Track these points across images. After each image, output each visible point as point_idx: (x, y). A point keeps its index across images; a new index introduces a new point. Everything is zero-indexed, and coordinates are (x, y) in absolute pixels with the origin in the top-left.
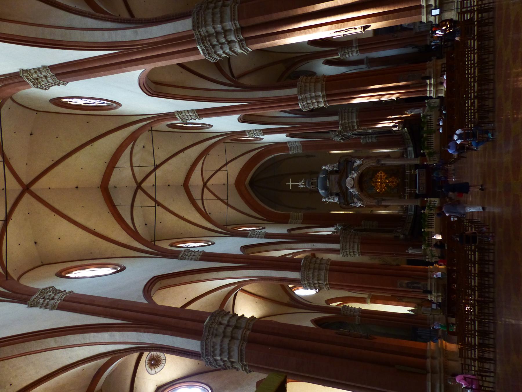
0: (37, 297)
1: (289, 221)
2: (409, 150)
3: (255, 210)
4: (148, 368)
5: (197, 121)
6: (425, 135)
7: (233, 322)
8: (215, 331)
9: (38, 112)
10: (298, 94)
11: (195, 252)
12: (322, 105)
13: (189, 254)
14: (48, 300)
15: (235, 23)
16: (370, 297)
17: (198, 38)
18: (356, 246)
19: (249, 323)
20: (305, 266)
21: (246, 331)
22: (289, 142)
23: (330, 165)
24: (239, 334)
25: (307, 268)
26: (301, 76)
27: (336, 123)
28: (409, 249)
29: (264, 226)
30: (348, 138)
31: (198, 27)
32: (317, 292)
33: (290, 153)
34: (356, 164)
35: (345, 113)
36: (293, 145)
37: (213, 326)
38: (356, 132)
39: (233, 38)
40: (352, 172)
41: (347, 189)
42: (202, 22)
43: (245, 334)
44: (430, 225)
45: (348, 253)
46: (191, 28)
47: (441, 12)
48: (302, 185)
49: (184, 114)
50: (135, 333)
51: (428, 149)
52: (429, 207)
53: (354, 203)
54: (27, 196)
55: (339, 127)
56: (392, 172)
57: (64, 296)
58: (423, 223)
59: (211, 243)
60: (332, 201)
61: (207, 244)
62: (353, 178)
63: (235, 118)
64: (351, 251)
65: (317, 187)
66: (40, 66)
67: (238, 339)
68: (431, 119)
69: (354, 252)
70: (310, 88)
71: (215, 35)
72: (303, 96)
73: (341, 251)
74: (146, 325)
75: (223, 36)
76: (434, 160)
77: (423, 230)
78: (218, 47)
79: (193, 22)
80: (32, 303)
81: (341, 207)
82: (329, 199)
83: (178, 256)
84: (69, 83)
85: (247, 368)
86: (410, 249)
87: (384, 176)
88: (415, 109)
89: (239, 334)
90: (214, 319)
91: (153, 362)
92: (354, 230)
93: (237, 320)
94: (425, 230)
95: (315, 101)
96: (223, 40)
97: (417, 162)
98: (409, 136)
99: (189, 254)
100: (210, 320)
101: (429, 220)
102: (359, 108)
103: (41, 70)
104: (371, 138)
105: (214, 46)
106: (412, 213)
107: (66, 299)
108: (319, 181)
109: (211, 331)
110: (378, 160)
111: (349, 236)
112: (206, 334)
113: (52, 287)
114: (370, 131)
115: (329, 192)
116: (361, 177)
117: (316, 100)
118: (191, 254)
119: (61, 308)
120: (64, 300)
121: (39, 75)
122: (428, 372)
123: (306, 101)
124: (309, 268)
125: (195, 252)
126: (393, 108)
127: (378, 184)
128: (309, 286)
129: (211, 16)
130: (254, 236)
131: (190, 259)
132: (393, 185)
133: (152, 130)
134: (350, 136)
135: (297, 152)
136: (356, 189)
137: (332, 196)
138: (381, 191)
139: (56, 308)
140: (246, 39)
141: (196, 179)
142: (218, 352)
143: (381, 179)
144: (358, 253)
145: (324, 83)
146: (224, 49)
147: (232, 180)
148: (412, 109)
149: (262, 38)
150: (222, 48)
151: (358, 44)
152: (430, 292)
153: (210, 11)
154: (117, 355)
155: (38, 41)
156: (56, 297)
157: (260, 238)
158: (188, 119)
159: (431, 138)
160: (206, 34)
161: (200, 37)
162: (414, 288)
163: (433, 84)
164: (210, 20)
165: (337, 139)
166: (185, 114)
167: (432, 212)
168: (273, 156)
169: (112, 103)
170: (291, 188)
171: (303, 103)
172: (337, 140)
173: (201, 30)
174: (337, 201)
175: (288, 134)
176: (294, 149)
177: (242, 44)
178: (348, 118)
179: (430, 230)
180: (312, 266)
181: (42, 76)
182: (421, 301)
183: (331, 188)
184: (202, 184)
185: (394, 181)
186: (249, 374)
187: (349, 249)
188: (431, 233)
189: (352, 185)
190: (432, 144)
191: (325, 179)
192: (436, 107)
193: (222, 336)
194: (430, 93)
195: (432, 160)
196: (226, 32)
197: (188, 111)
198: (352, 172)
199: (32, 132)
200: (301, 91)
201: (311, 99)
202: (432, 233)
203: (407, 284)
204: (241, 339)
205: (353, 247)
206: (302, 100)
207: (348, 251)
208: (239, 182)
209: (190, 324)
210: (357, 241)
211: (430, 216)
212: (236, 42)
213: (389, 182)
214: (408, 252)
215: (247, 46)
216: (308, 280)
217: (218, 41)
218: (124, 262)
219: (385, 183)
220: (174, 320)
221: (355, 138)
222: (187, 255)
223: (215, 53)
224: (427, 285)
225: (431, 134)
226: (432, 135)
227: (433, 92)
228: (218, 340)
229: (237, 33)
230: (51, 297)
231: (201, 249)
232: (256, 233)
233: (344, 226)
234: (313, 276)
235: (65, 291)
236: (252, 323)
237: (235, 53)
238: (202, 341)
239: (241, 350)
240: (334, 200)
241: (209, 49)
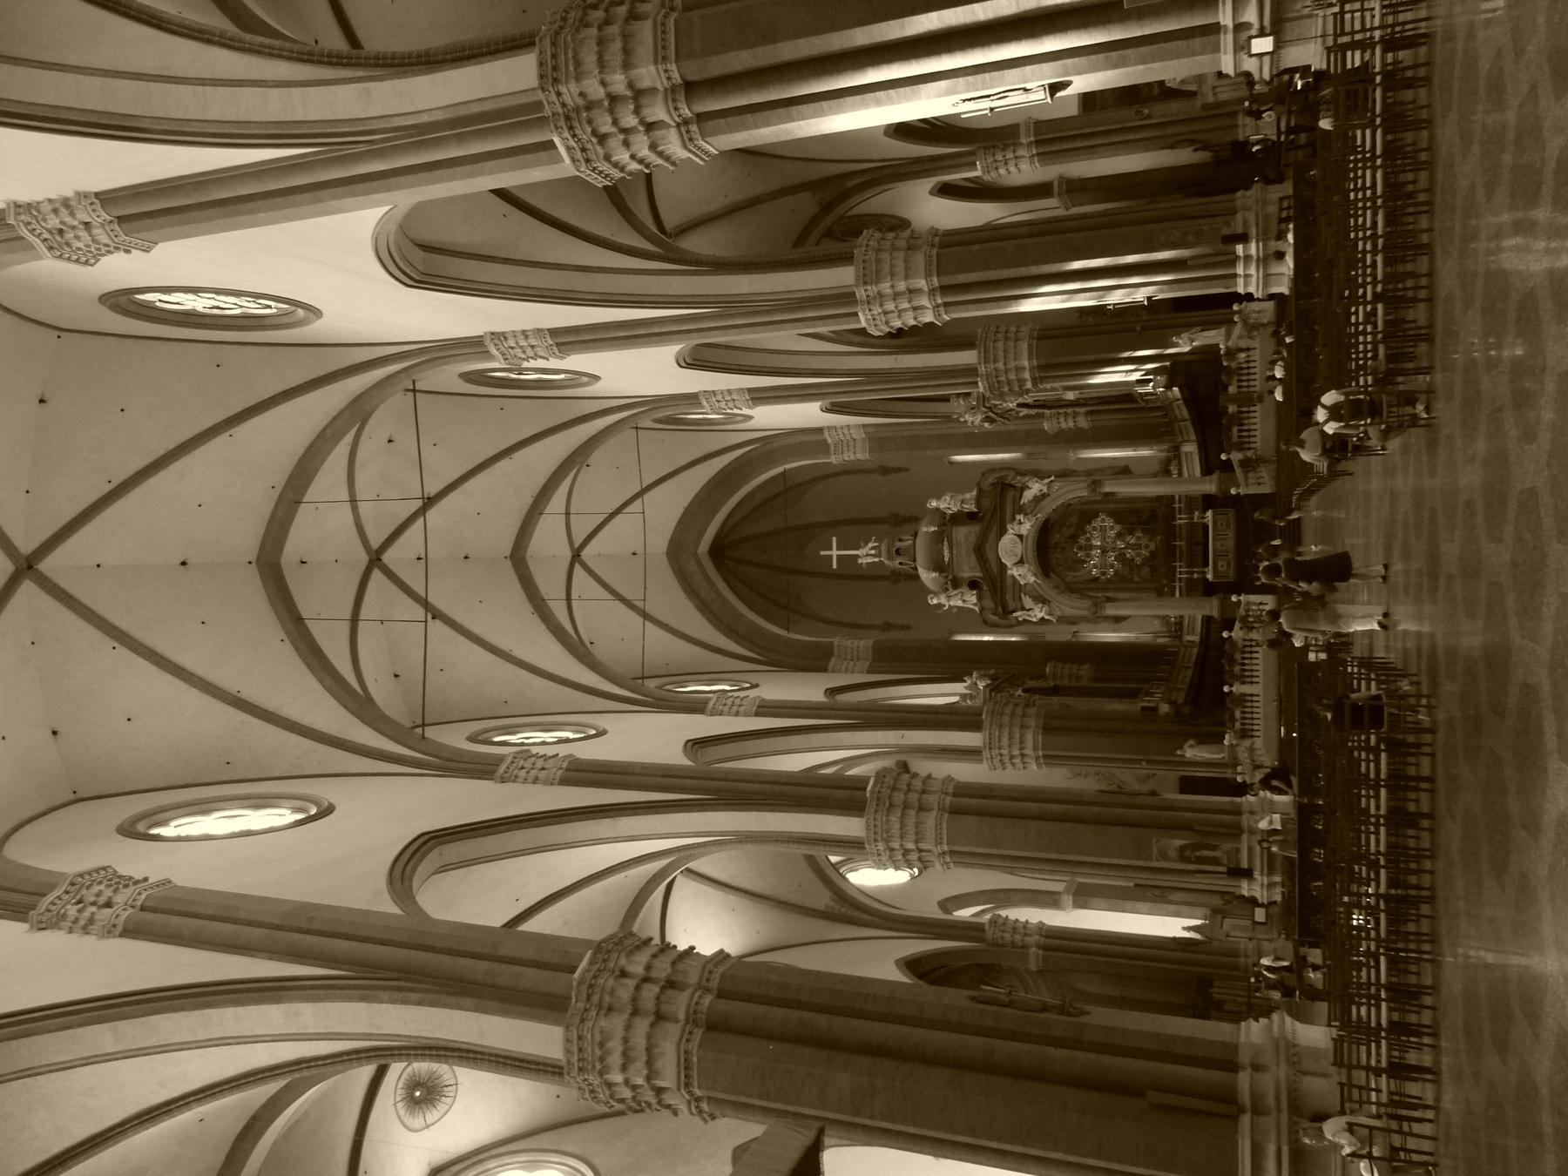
0: (59, 898)
1: (831, 664)
2: (1186, 453)
3: (729, 631)
4: (402, 1112)
5: (553, 363)
6: (1232, 409)
7: (662, 969)
8: (607, 998)
9: (62, 334)
10: (857, 285)
11: (545, 760)
12: (928, 317)
13: (528, 764)
14: (93, 909)
15: (666, 71)
16: (1073, 890)
17: (554, 114)
18: (1029, 737)
19: (710, 972)
20: (878, 799)
21: (700, 997)
22: (829, 428)
23: (952, 497)
24: (680, 1004)
26: (865, 231)
27: (970, 371)
28: (1186, 746)
29: (754, 678)
30: (1005, 415)
31: (556, 81)
32: (913, 878)
33: (833, 459)
34: (1028, 496)
35: (995, 341)
36: (842, 437)
37: (602, 981)
38: (1029, 399)
39: (657, 111)
40: (1018, 517)
41: (1003, 567)
42: (567, 68)
43: (697, 1003)
44: (1247, 674)
45: (1006, 759)
46: (535, 83)
47: (1278, 45)
48: (868, 555)
49: (512, 343)
50: (362, 1006)
51: (1241, 449)
52: (1244, 620)
53: (1023, 609)
54: (28, 588)
55: (980, 384)
56: (1137, 516)
57: (143, 896)
58: (1227, 669)
59: (594, 732)
60: (960, 603)
61: (582, 735)
62: (1020, 537)
63: (668, 353)
64: (1016, 752)
65: (915, 561)
66: (70, 194)
67: (677, 1021)
68: (1248, 362)
69: (1023, 755)
70: (892, 266)
71: (606, 103)
72: (873, 289)
73: (986, 754)
74: (398, 980)
75: (632, 107)
76: (1259, 481)
77: (1226, 689)
78: (615, 142)
79: (541, 64)
80: (44, 919)
81: (985, 622)
82: (949, 597)
83: (495, 772)
84: (161, 245)
85: (705, 1106)
86: (1191, 746)
87: (1112, 528)
88: (1202, 331)
89: (680, 1004)
90: (605, 961)
91: (418, 1094)
92: (1024, 691)
93: (673, 964)
94: (1234, 689)
95: (905, 305)
96: (630, 120)
97: (1210, 486)
98: (1185, 413)
99: (528, 764)
100: (591, 963)
101: (1244, 658)
102: (1037, 328)
103: (72, 203)
104: (1074, 418)
105: (603, 139)
106: (1196, 638)
107: (150, 904)
108: (919, 541)
109: (595, 998)
110: (1094, 482)
111: (1008, 710)
112: (581, 1005)
113: (104, 868)
114: (1070, 396)
115: (950, 577)
116: (1045, 532)
117: (910, 302)
118: (534, 764)
119: (132, 931)
120: (143, 909)
121: (68, 220)
122: (1242, 1110)
123: (881, 305)
124: (891, 806)
125: (545, 760)
126: (1138, 328)
127: (1093, 552)
128: (891, 857)
129: (596, 48)
130: (726, 709)
131: (530, 780)
132: (1138, 555)
133: (414, 391)
134: (1011, 410)
135: (852, 458)
136: (1029, 570)
137: (959, 590)
138: (1104, 574)
139: (117, 933)
140: (701, 118)
141: (549, 540)
142: (615, 1059)
143: (1103, 538)
144: (1037, 758)
145: (935, 251)
146: (634, 148)
147: (659, 542)
148: (1195, 330)
149: (749, 116)
150: (626, 144)
151: (1035, 135)
152: (1248, 874)
153: (593, 31)
154: (306, 1073)
155: (64, 115)
156: (119, 899)
158: (523, 356)
159: (1249, 418)
160: (580, 102)
161: (560, 111)
162: (1200, 860)
163: (1255, 258)
164: (590, 59)
165: (974, 419)
166: (517, 343)
167: (1254, 635)
168: (781, 469)
169: (293, 308)
170: (835, 566)
171: (870, 310)
172: (973, 422)
173: (563, 89)
174: (975, 604)
175: (827, 402)
176: (845, 449)
177: (688, 132)
178: (1005, 357)
180: (899, 797)
181: (75, 223)
182: (1223, 899)
183: (955, 564)
184: (568, 554)
185: (1140, 545)
186: (711, 1122)
187: (1010, 746)
188: (1249, 698)
189: (1015, 555)
190: (1253, 433)
191: (938, 538)
192: (1263, 325)
193: (629, 1010)
194: (1246, 285)
195: (1251, 481)
196: (639, 95)
197: (524, 332)
198: (1018, 517)
199: (43, 395)
200: (864, 275)
201: (894, 299)
202: (1255, 698)
203: (1182, 849)
204: (687, 1019)
205: (1021, 742)
206: (869, 303)
207: (1005, 752)
208: (677, 550)
210: (1032, 723)
211: (1248, 649)
212: (669, 126)
213: (1128, 546)
214: (1183, 756)
215: (703, 140)
216: (887, 841)
217: (615, 122)
218: (326, 791)
219: (1114, 549)
220: (484, 965)
221: (1026, 417)
222: (522, 768)
223: (607, 158)
224: (1238, 851)
225: (1249, 406)
226: (1252, 409)
227: (1254, 280)
228: (616, 1023)
229: (674, 100)
230: (102, 900)
231: (563, 750)
232: (729, 701)
233: (993, 679)
234: (903, 825)
235: (146, 879)
236: (721, 970)
237: (667, 159)
238: (567, 1028)
239: (686, 1052)
240: (964, 601)
241: (589, 146)
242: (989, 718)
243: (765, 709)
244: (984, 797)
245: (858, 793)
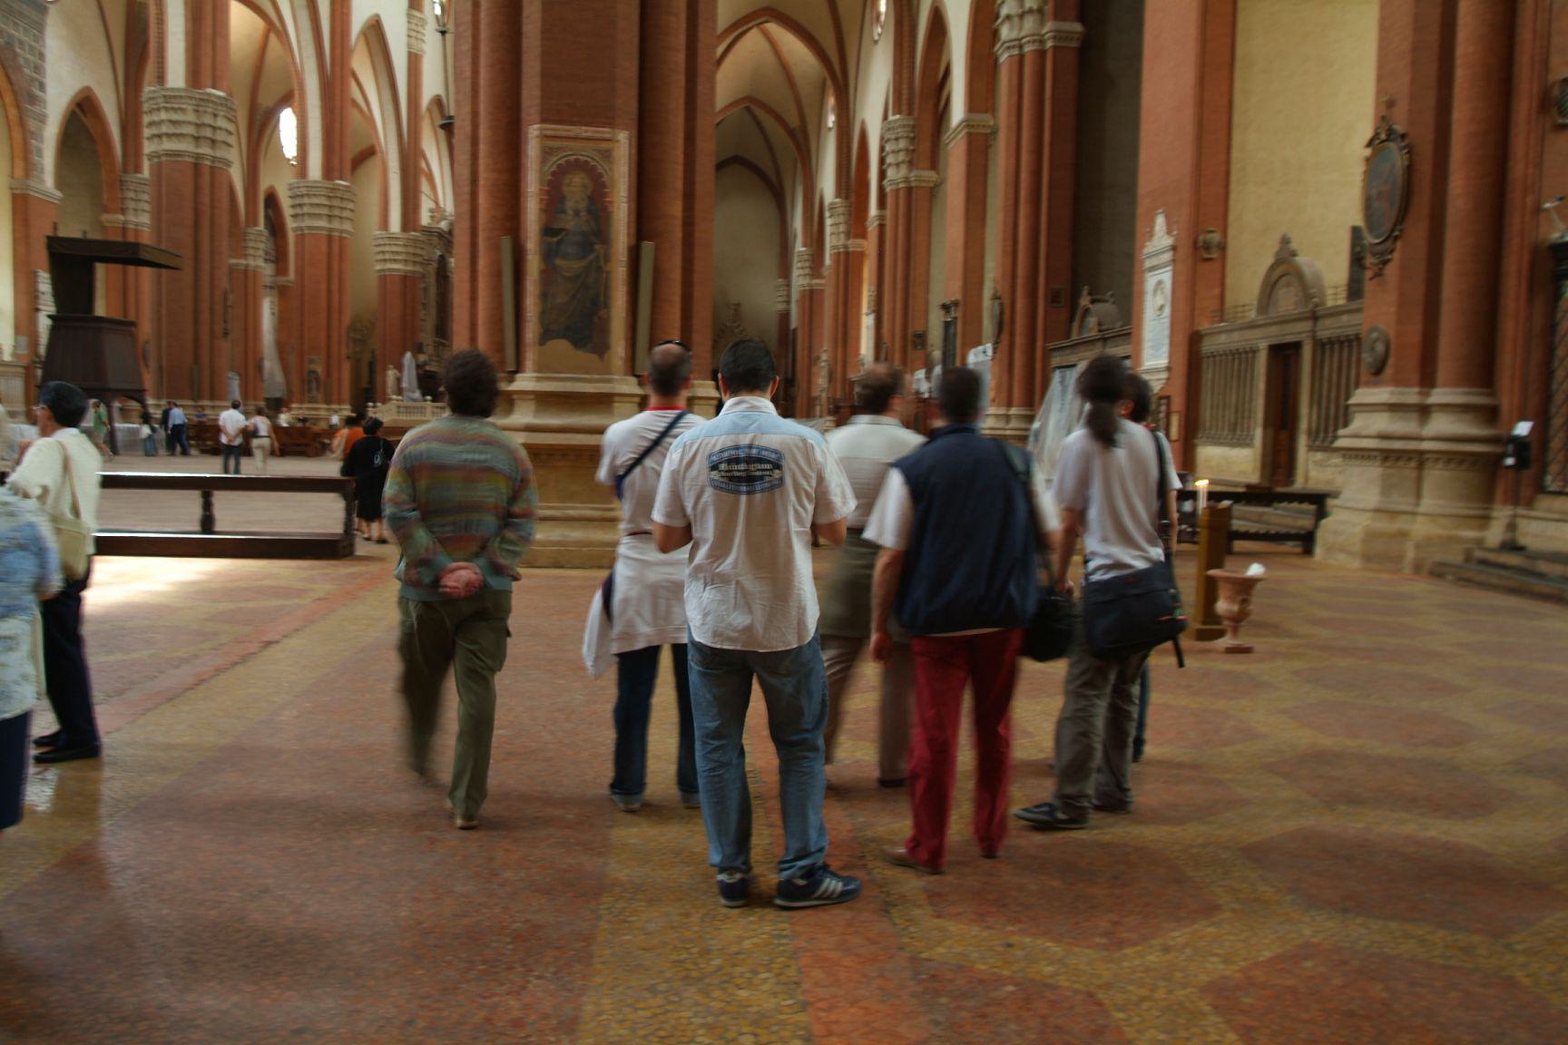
89: (205, 150)
100: (220, 97)
112: (197, 96)
130: (414, 27)
144: (383, 270)
157: (408, 41)
179: (429, 410)
180: (336, 203)
193: (198, 122)
203: (314, 372)
209: (206, 62)
210: (410, 268)
214: (389, 369)
224: (316, 402)
228: (191, 117)
234: (318, 205)
238: (184, 90)
242: (411, 237)
243: (414, 61)
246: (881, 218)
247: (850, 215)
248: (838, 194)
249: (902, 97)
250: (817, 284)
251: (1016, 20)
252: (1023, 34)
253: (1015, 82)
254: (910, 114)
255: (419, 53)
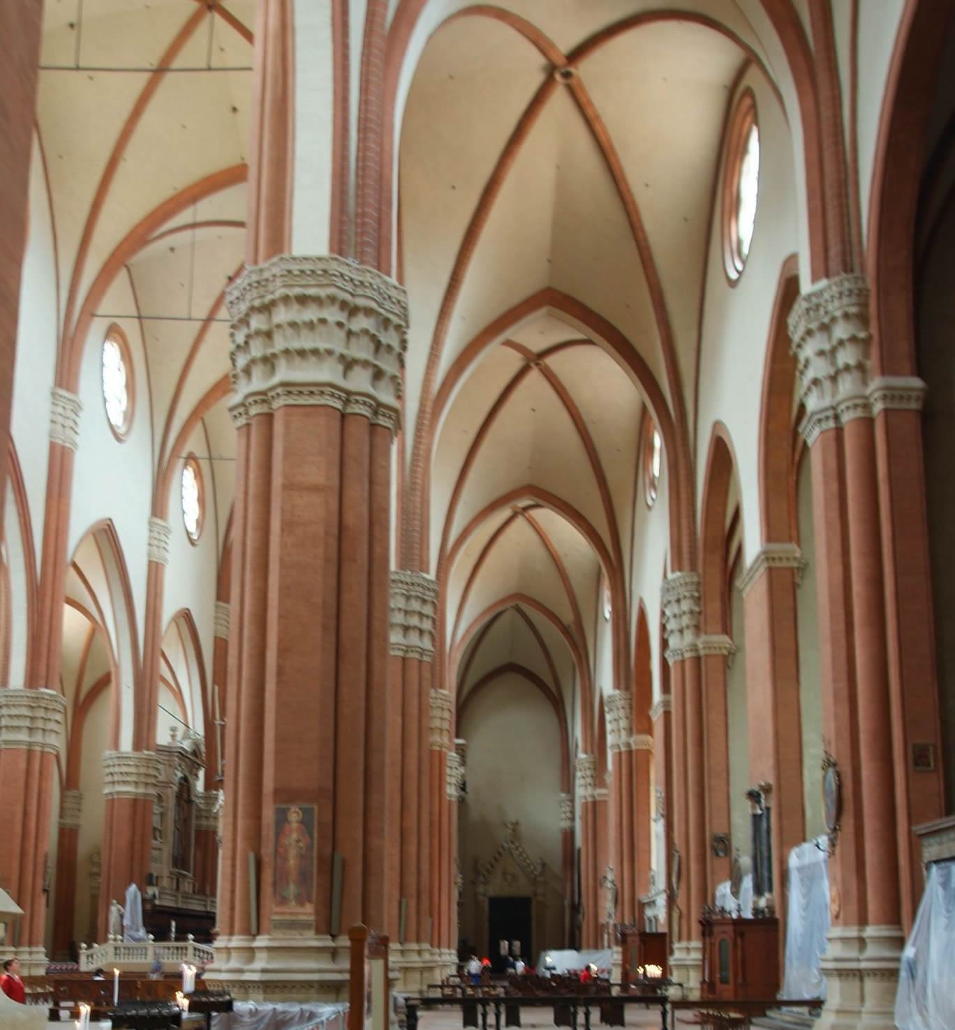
20: (37, 698)
25: (34, 702)
73: (113, 753)
124: (32, 707)
130: (156, 535)
177: (827, 418)
180: (41, 713)
223: (809, 333)
243: (155, 571)
244: (41, 773)
245: (42, 682)
246: (666, 704)
247: (631, 708)
248: (617, 685)
249: (681, 554)
250: (599, 795)
251: (827, 384)
252: (840, 397)
253: (833, 464)
254: (693, 568)
255: (160, 561)
